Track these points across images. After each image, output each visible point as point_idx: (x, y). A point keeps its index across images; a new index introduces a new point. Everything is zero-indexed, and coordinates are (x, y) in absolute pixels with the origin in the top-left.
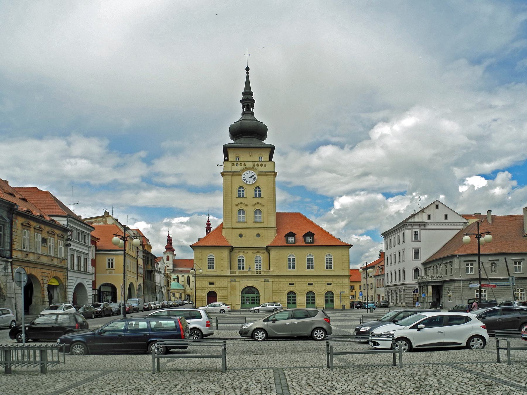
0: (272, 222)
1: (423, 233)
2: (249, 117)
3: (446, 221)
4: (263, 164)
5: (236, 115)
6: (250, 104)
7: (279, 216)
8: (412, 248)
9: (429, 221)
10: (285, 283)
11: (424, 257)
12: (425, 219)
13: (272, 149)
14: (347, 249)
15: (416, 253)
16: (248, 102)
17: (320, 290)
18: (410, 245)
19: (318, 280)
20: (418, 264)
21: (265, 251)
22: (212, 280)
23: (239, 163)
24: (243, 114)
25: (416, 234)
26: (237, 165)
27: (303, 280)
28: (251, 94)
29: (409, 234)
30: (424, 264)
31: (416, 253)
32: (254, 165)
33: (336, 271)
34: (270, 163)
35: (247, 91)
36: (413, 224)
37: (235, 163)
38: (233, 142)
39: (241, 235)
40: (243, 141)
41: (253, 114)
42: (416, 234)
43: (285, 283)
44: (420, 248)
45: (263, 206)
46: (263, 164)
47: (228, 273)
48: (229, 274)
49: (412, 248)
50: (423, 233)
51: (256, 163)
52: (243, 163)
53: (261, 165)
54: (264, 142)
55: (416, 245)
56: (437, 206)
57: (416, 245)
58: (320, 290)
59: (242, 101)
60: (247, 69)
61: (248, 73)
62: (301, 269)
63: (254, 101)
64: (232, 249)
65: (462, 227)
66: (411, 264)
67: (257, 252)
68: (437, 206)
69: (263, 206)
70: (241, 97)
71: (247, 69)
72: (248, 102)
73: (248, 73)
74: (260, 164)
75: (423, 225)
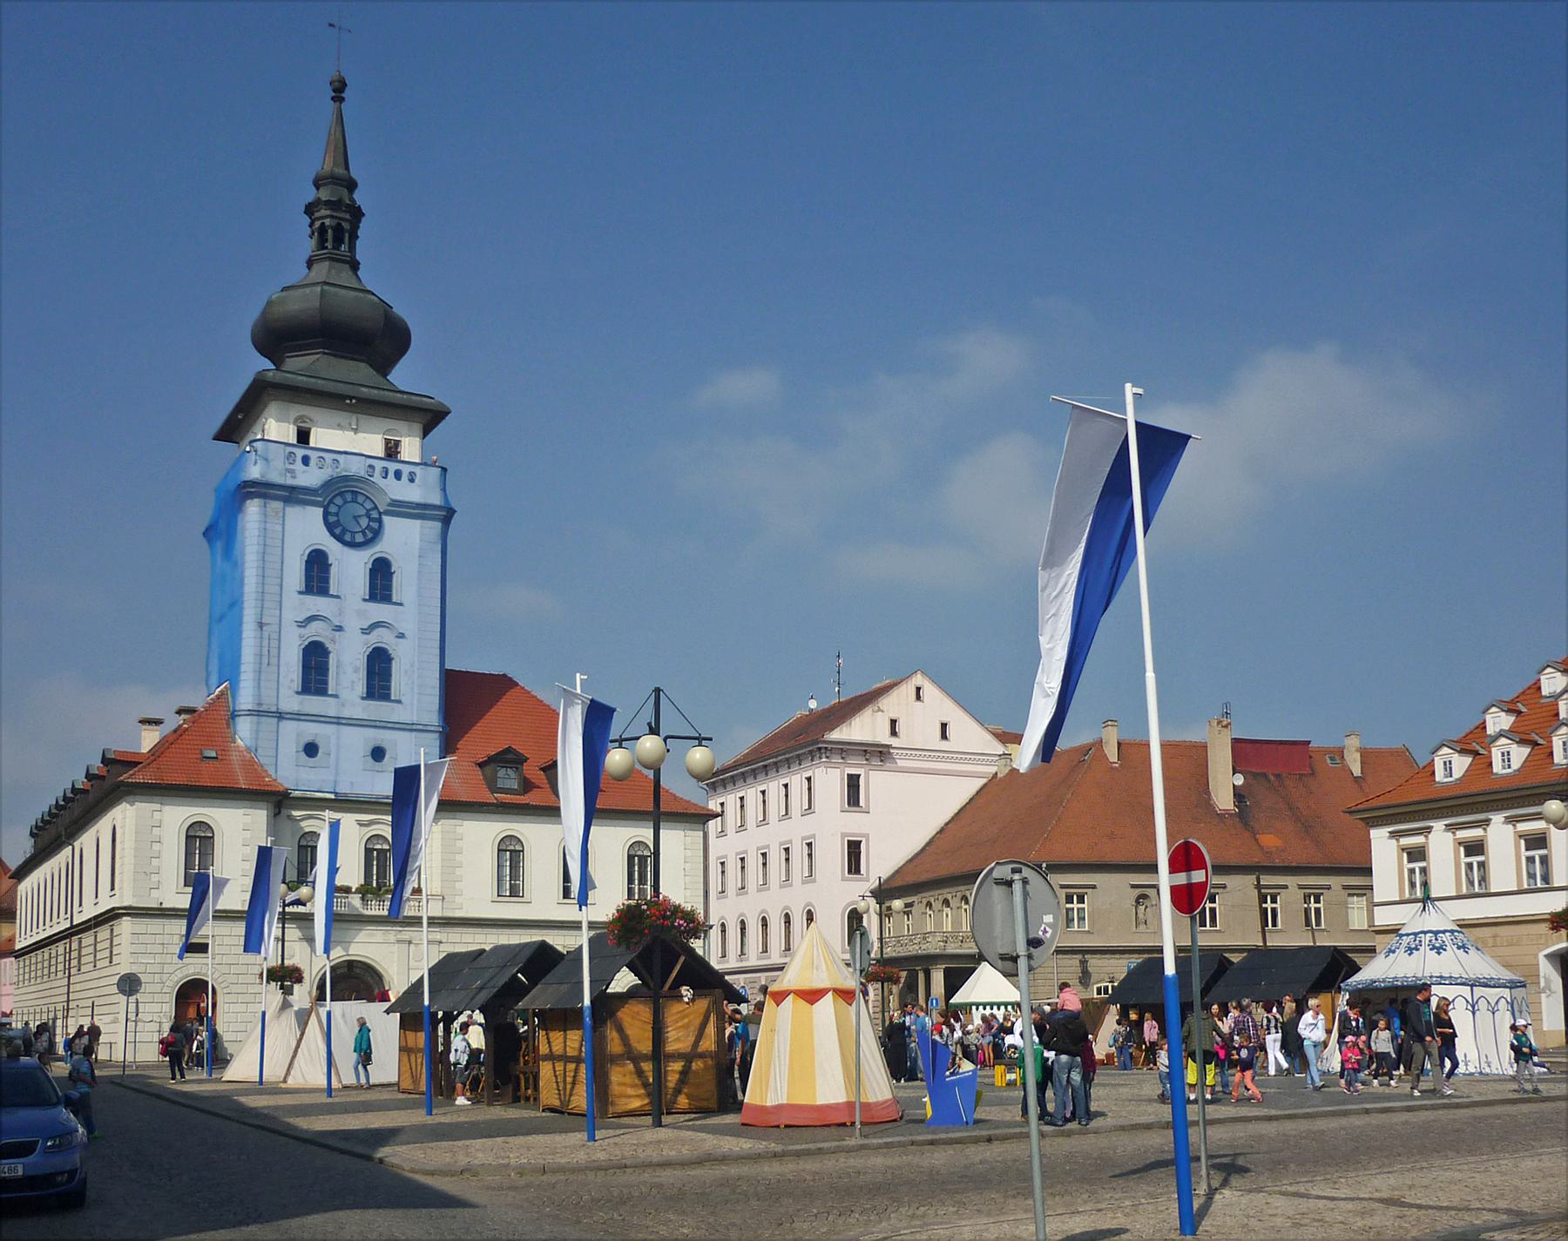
1: (876, 782)
3: (944, 745)
4: (406, 469)
6: (346, 226)
8: (843, 835)
9: (894, 742)
11: (882, 863)
12: (884, 737)
15: (854, 849)
18: (831, 823)
20: (857, 892)
25: (853, 783)
28: (351, 185)
29: (829, 779)
30: (883, 893)
31: (854, 849)
35: (340, 171)
36: (846, 750)
39: (311, 749)
41: (355, 266)
42: (853, 783)
44: (867, 836)
45: (401, 636)
46: (406, 469)
49: (843, 835)
50: (876, 782)
55: (854, 824)
56: (918, 689)
57: (854, 824)
61: (338, 97)
65: (993, 769)
66: (838, 894)
67: (371, 823)
68: (918, 689)
69: (401, 636)
73: (338, 97)
74: (393, 466)
75: (878, 753)
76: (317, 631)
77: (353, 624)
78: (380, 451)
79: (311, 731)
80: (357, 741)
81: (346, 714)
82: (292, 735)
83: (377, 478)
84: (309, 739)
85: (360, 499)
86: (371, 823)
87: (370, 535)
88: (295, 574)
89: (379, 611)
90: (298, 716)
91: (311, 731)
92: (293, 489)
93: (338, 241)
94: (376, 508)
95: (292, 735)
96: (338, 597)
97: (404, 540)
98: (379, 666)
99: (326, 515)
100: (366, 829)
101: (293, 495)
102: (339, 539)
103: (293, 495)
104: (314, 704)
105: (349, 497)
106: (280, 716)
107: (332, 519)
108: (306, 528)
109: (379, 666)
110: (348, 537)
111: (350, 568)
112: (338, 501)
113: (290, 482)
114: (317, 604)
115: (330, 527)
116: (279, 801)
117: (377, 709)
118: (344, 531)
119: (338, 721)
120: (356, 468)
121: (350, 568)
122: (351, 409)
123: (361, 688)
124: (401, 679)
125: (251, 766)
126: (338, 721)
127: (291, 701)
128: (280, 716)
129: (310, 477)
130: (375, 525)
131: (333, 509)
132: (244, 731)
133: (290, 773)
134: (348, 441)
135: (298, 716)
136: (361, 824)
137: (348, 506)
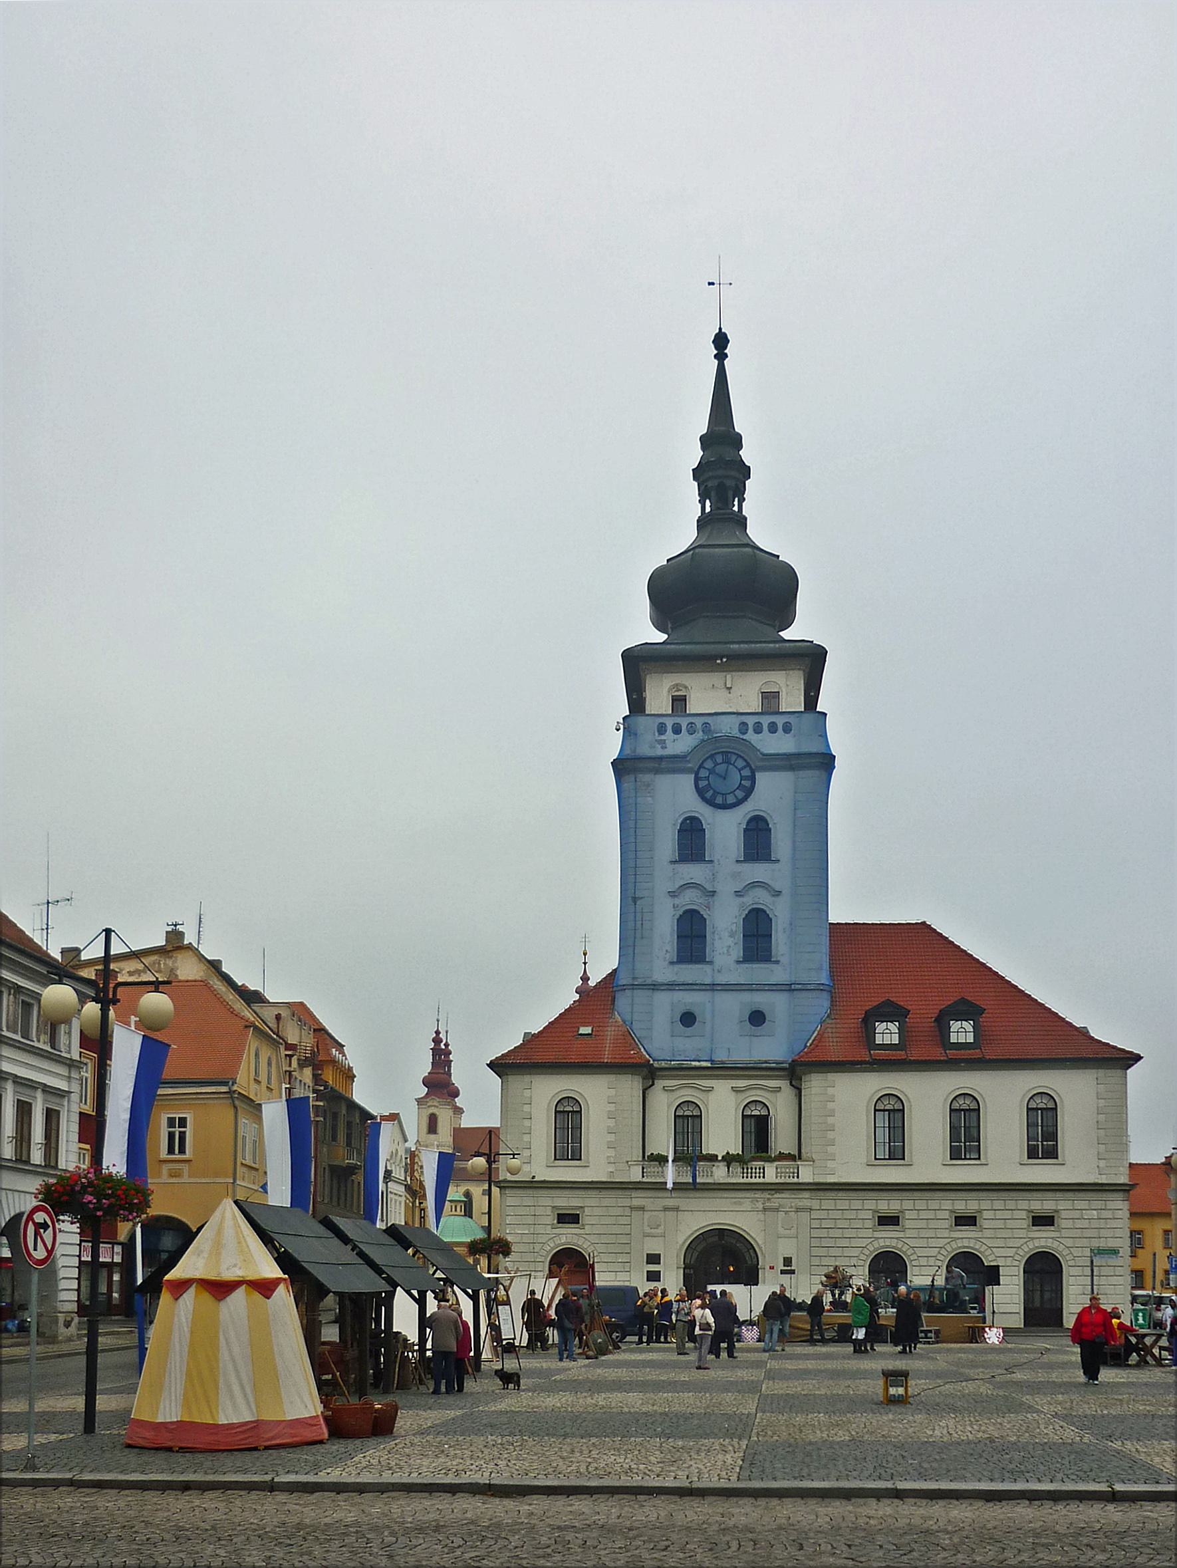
0: (814, 965)
5: (677, 527)
6: (730, 483)
7: (848, 937)
10: (863, 1215)
13: (812, 660)
14: (1119, 1072)
16: (722, 470)
17: (1006, 1244)
19: (998, 1205)
21: (784, 1084)
22: (567, 1201)
23: (684, 722)
24: (702, 523)
26: (677, 730)
27: (934, 1205)
32: (743, 727)
33: (1077, 1163)
34: (810, 716)
37: (669, 723)
38: (661, 637)
39: (688, 1019)
41: (742, 522)
43: (863, 1215)
45: (778, 893)
46: (780, 721)
47: (636, 1175)
48: (639, 1179)
51: (751, 721)
52: (699, 722)
53: (773, 728)
54: (786, 634)
58: (1006, 1244)
59: (697, 473)
60: (721, 341)
61: (721, 356)
62: (929, 1157)
63: (746, 472)
64: (649, 1073)
67: (749, 1088)
69: (778, 893)
70: (695, 454)
71: (721, 341)
72: (722, 470)
73: (721, 356)
74: (765, 721)
76: (690, 899)
77: (726, 888)
78: (755, 705)
79: (689, 999)
80: (733, 1006)
81: (722, 979)
82: (665, 1006)
83: (750, 736)
84: (683, 1009)
85: (734, 758)
86: (749, 1088)
87: (740, 794)
89: (759, 871)
90: (671, 986)
91: (689, 999)
92: (661, 758)
94: (748, 765)
95: (665, 1006)
96: (711, 861)
99: (697, 780)
100: (741, 1096)
102: (711, 803)
104: (690, 972)
105: (719, 759)
106: (655, 987)
107: (702, 784)
110: (719, 800)
111: (725, 831)
112: (709, 764)
113: (659, 752)
114: (693, 872)
115: (700, 792)
118: (716, 793)
119: (713, 987)
120: (728, 727)
121: (725, 831)
122: (723, 669)
123: (737, 952)
124: (780, 941)
125: (628, 1038)
126: (713, 987)
127: (662, 971)
128: (655, 987)
129: (680, 744)
130: (747, 783)
131: (703, 773)
133: (660, 1039)
135: (671, 986)
136: (735, 1090)
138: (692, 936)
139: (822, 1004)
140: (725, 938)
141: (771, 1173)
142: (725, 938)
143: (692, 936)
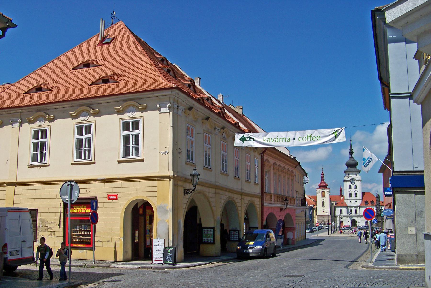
2: (352, 159)
40: (350, 168)
41: (353, 157)
60: (351, 141)
71: (351, 141)
76: (350, 192)
88: (348, 187)
93: (351, 155)
95: (349, 201)
97: (357, 183)
98: (356, 194)
101: (348, 181)
103: (348, 181)
104: (351, 198)
108: (349, 183)
109: (356, 194)
111: (353, 186)
116: (347, 207)
117: (356, 198)
121: (353, 186)
132: (345, 200)
134: (352, 176)
137: (353, 181)
138: (350, 195)
139: (361, 200)
140: (353, 195)
141: (358, 215)
142: (353, 195)
143: (350, 195)
